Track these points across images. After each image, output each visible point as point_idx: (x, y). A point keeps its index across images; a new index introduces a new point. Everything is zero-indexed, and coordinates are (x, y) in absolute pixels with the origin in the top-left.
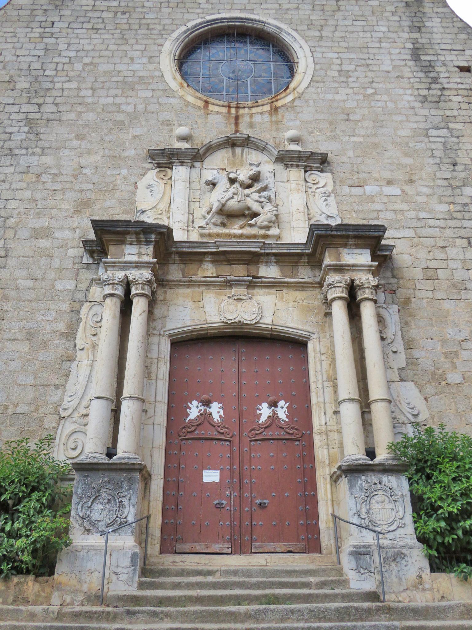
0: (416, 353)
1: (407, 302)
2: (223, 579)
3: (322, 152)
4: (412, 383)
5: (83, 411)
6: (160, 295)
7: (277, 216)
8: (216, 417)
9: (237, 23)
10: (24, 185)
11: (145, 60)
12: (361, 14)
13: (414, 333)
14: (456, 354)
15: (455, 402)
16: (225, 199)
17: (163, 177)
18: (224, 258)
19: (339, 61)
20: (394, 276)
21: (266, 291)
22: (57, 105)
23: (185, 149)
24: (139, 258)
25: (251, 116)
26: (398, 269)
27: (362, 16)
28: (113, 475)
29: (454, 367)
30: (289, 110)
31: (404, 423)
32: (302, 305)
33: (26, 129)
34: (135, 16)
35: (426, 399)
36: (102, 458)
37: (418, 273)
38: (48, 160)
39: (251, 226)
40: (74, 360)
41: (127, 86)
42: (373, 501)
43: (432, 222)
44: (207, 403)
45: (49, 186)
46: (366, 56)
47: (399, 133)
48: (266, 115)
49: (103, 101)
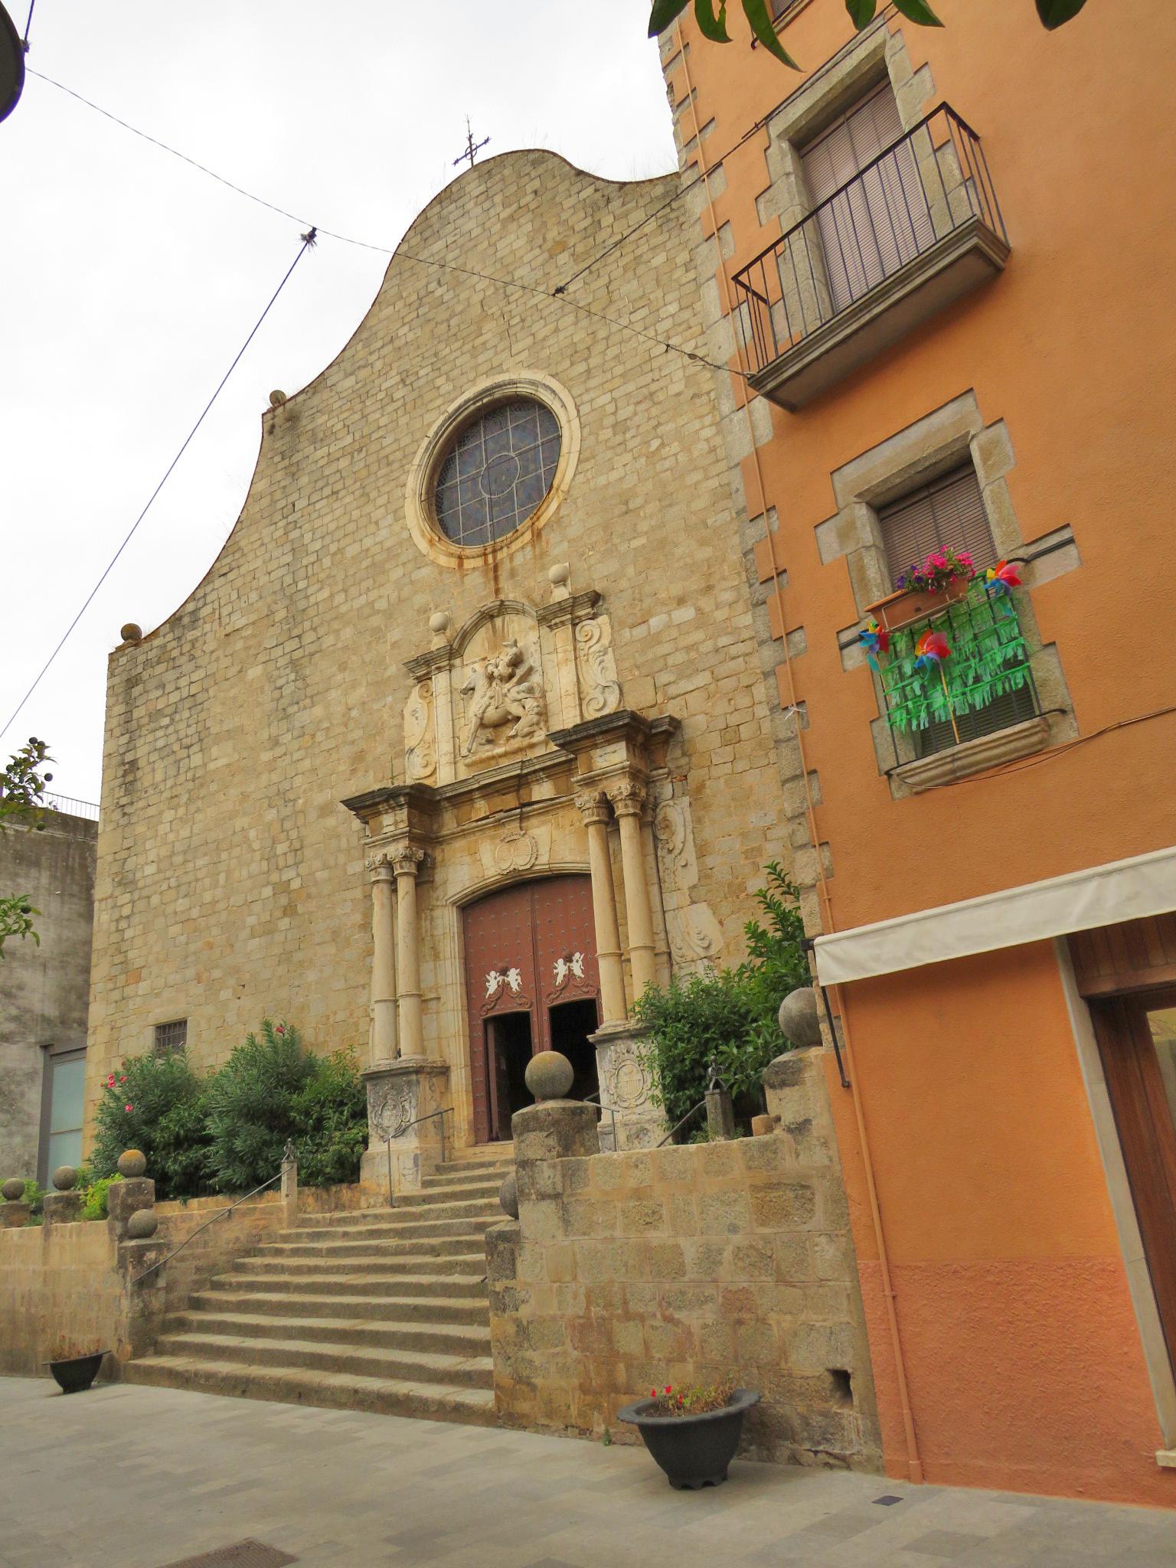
0: (710, 861)
1: (701, 788)
8: (514, 986)
10: (302, 753)
11: (390, 519)
13: (708, 832)
18: (488, 790)
19: (610, 408)
20: (684, 754)
21: (542, 818)
22: (314, 629)
25: (511, 557)
27: (641, 298)
28: (395, 1080)
33: (292, 676)
34: (373, 447)
35: (721, 923)
37: (714, 739)
38: (318, 711)
39: (513, 737)
41: (378, 569)
43: (733, 651)
44: (504, 972)
45: (325, 746)
46: (648, 378)
48: (529, 548)
49: (357, 604)
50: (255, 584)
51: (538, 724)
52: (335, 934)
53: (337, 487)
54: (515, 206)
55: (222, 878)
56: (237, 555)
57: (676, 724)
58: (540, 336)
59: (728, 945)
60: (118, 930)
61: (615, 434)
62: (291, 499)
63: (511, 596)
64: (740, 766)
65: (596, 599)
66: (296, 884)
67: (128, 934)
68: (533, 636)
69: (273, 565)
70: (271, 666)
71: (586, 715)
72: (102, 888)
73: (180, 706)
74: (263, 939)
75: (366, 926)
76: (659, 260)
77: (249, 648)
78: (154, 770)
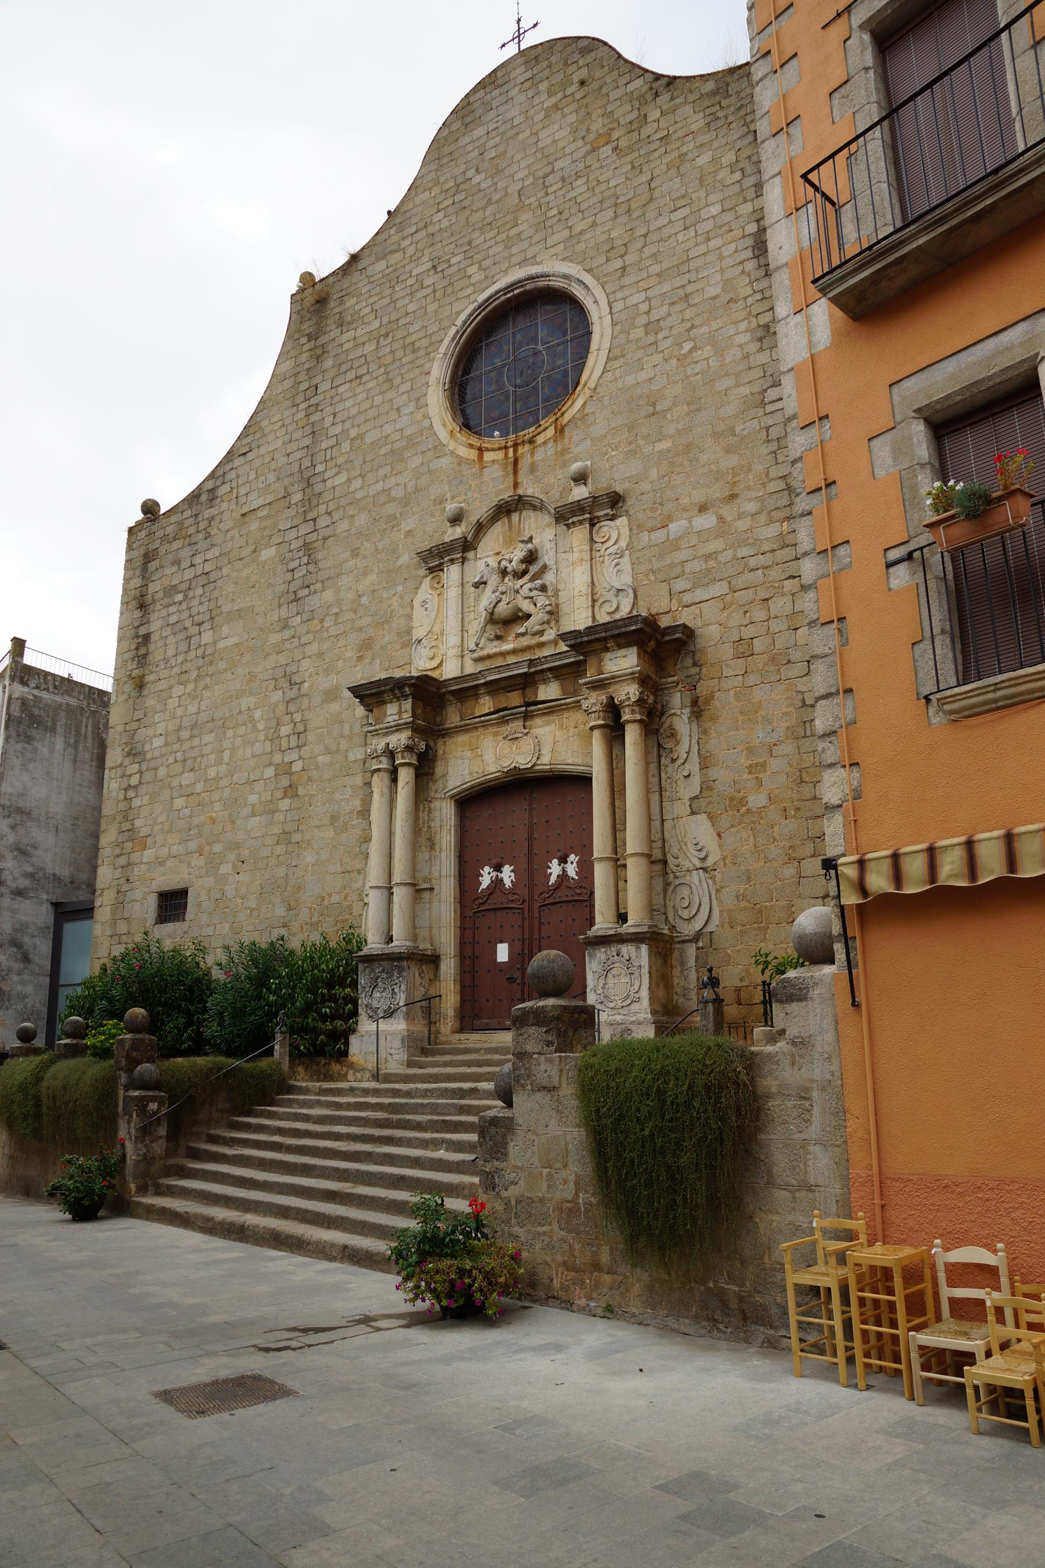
0: (712, 773)
2: (486, 1057)
7: (550, 613)
8: (508, 883)
9: (516, 292)
10: (311, 637)
11: (412, 406)
12: (683, 192)
14: (764, 766)
15: (754, 835)
18: (495, 687)
19: (644, 307)
20: (695, 664)
21: (546, 718)
22: (329, 514)
25: (532, 454)
26: (701, 651)
27: (683, 196)
29: (759, 783)
30: (579, 423)
33: (305, 560)
34: (400, 334)
35: (719, 835)
37: (727, 651)
38: (328, 596)
39: (523, 635)
41: (397, 456)
42: (610, 975)
43: (753, 562)
44: (498, 868)
47: (722, 412)
49: (373, 491)
50: (273, 465)
51: (548, 623)
52: (334, 819)
53: (361, 372)
54: (560, 95)
55: (226, 755)
56: (257, 436)
57: (689, 633)
58: (577, 229)
59: (725, 858)
60: (125, 799)
61: (647, 334)
62: (313, 383)
63: (530, 492)
64: (752, 679)
65: (615, 500)
66: (297, 767)
67: (136, 803)
68: (549, 534)
69: (294, 446)
70: (284, 548)
71: (598, 617)
72: (114, 756)
73: (194, 583)
74: (263, 818)
75: (365, 813)
76: (704, 159)
77: (265, 528)
78: (165, 645)
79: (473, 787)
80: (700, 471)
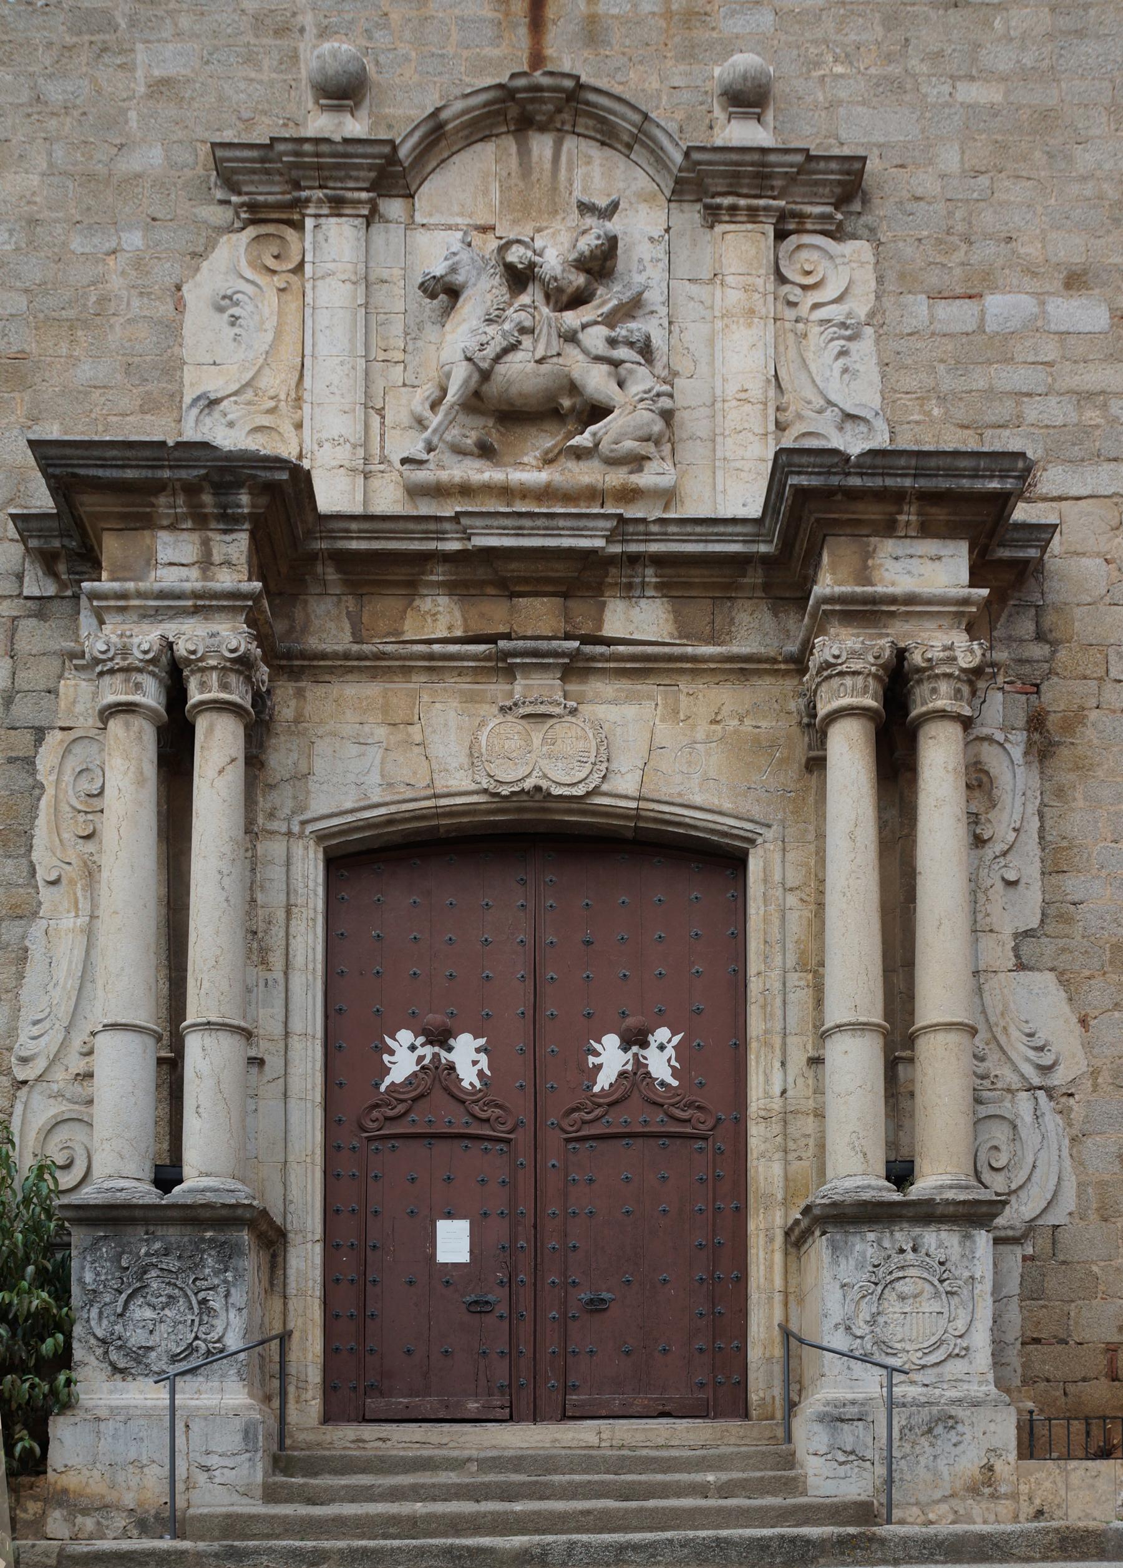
3: (846, 151)
4: (1050, 976)
5: (78, 1065)
6: (285, 707)
7: (667, 416)
8: (468, 1076)
16: (490, 352)
17: (271, 263)
18: (486, 574)
21: (625, 685)
23: (346, 141)
24: (205, 578)
31: (1009, 1090)
32: (736, 732)
36: (146, 1193)
40: (35, 914)
44: (441, 1037)
79: (390, 821)
80: (1074, 189)
